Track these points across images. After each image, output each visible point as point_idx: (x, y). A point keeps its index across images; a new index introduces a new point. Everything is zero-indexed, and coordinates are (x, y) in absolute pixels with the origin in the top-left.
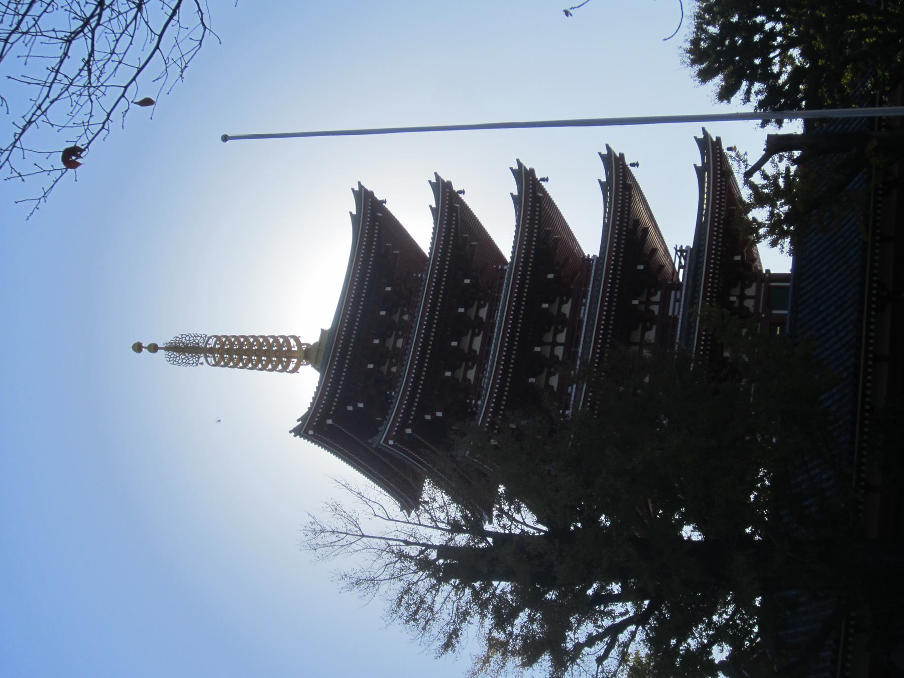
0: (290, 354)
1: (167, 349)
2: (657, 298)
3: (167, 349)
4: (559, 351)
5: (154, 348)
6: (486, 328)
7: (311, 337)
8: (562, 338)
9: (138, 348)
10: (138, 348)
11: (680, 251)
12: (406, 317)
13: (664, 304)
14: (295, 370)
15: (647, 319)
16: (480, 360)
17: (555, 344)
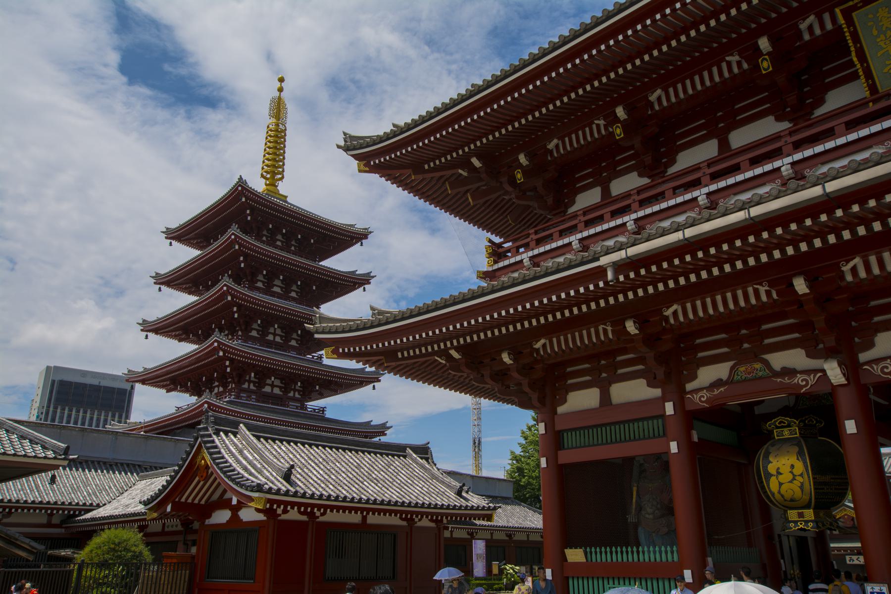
0: (274, 174)
1: (280, 98)
2: (297, 395)
3: (280, 98)
4: (270, 337)
5: (281, 90)
6: (285, 296)
7: (283, 188)
8: (278, 339)
9: (281, 80)
10: (281, 80)
11: (323, 410)
12: (293, 248)
13: (294, 399)
14: (262, 176)
15: (286, 389)
16: (268, 291)
17: (275, 335)
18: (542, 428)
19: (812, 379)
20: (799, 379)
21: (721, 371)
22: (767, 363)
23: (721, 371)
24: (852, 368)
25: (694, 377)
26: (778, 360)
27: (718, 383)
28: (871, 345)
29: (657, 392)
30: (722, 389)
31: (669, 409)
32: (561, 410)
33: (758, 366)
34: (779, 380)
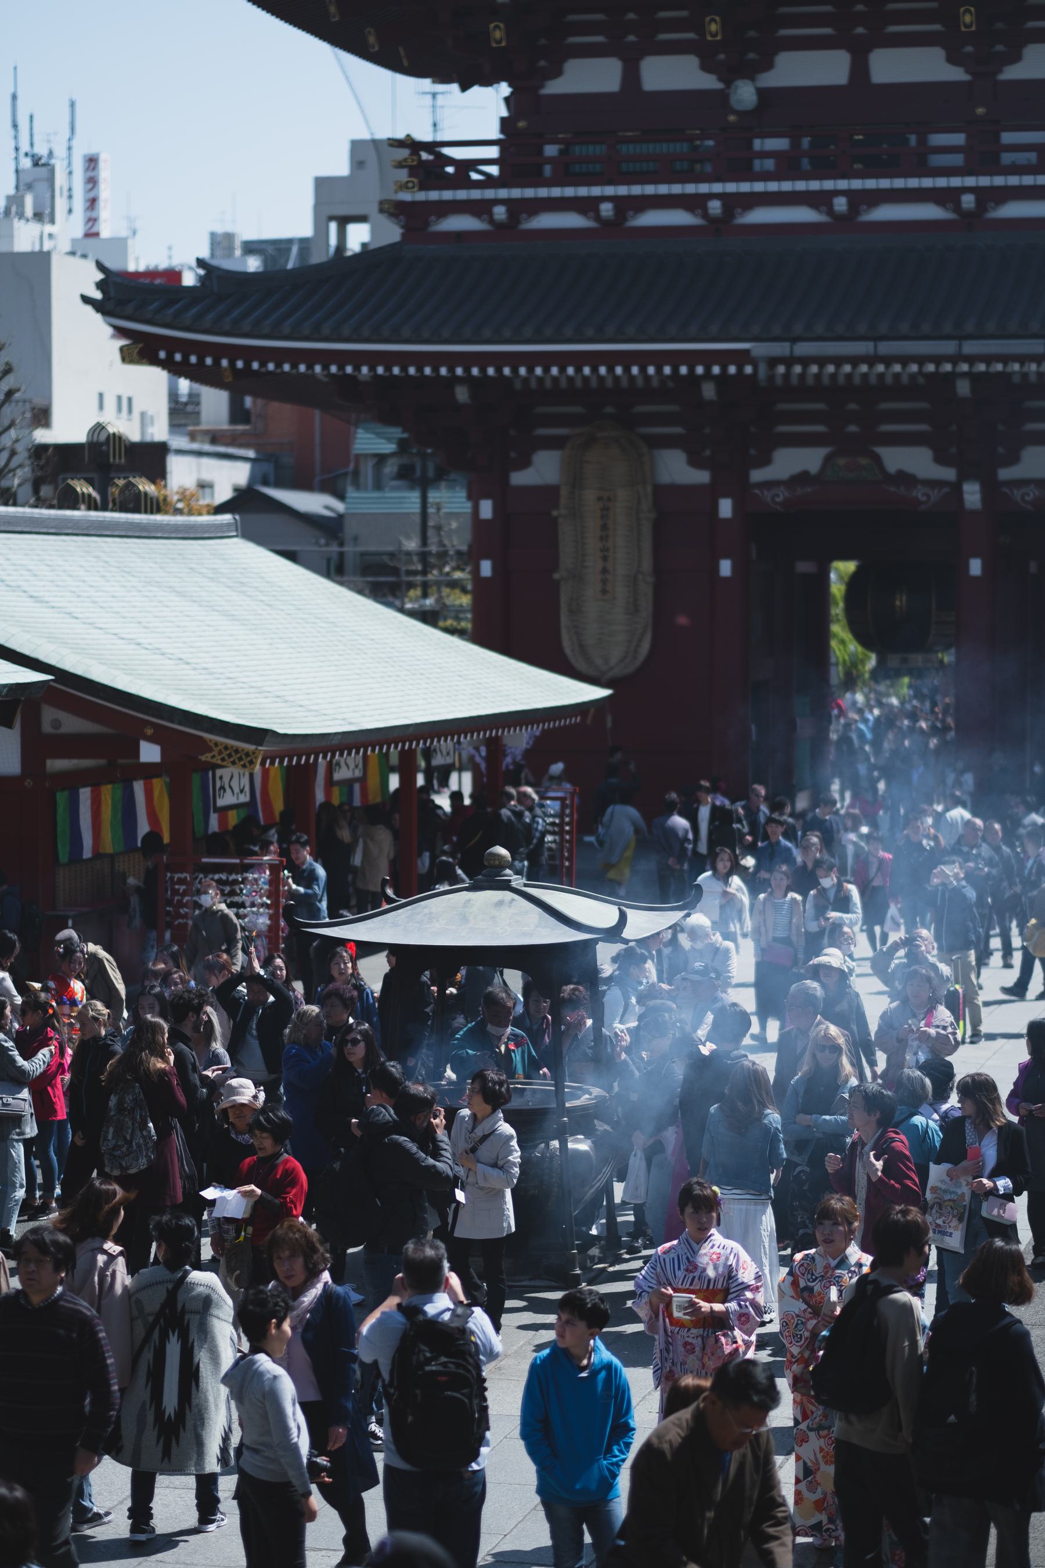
18: (486, 509)
19: (935, 494)
20: (919, 493)
21: (808, 460)
22: (877, 459)
23: (808, 460)
24: (992, 489)
25: (765, 461)
26: (898, 459)
27: (802, 478)
28: (1013, 459)
29: (703, 477)
30: (809, 490)
31: (726, 508)
32: (519, 478)
33: (864, 461)
34: (892, 489)
